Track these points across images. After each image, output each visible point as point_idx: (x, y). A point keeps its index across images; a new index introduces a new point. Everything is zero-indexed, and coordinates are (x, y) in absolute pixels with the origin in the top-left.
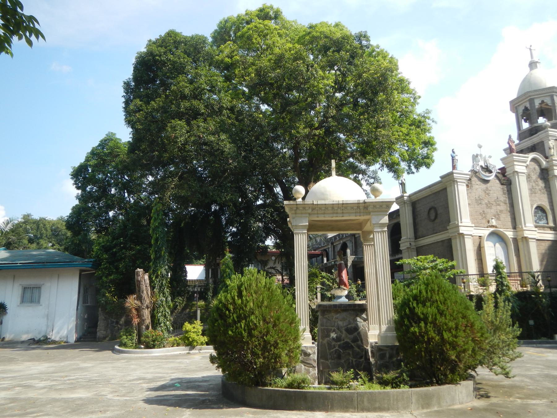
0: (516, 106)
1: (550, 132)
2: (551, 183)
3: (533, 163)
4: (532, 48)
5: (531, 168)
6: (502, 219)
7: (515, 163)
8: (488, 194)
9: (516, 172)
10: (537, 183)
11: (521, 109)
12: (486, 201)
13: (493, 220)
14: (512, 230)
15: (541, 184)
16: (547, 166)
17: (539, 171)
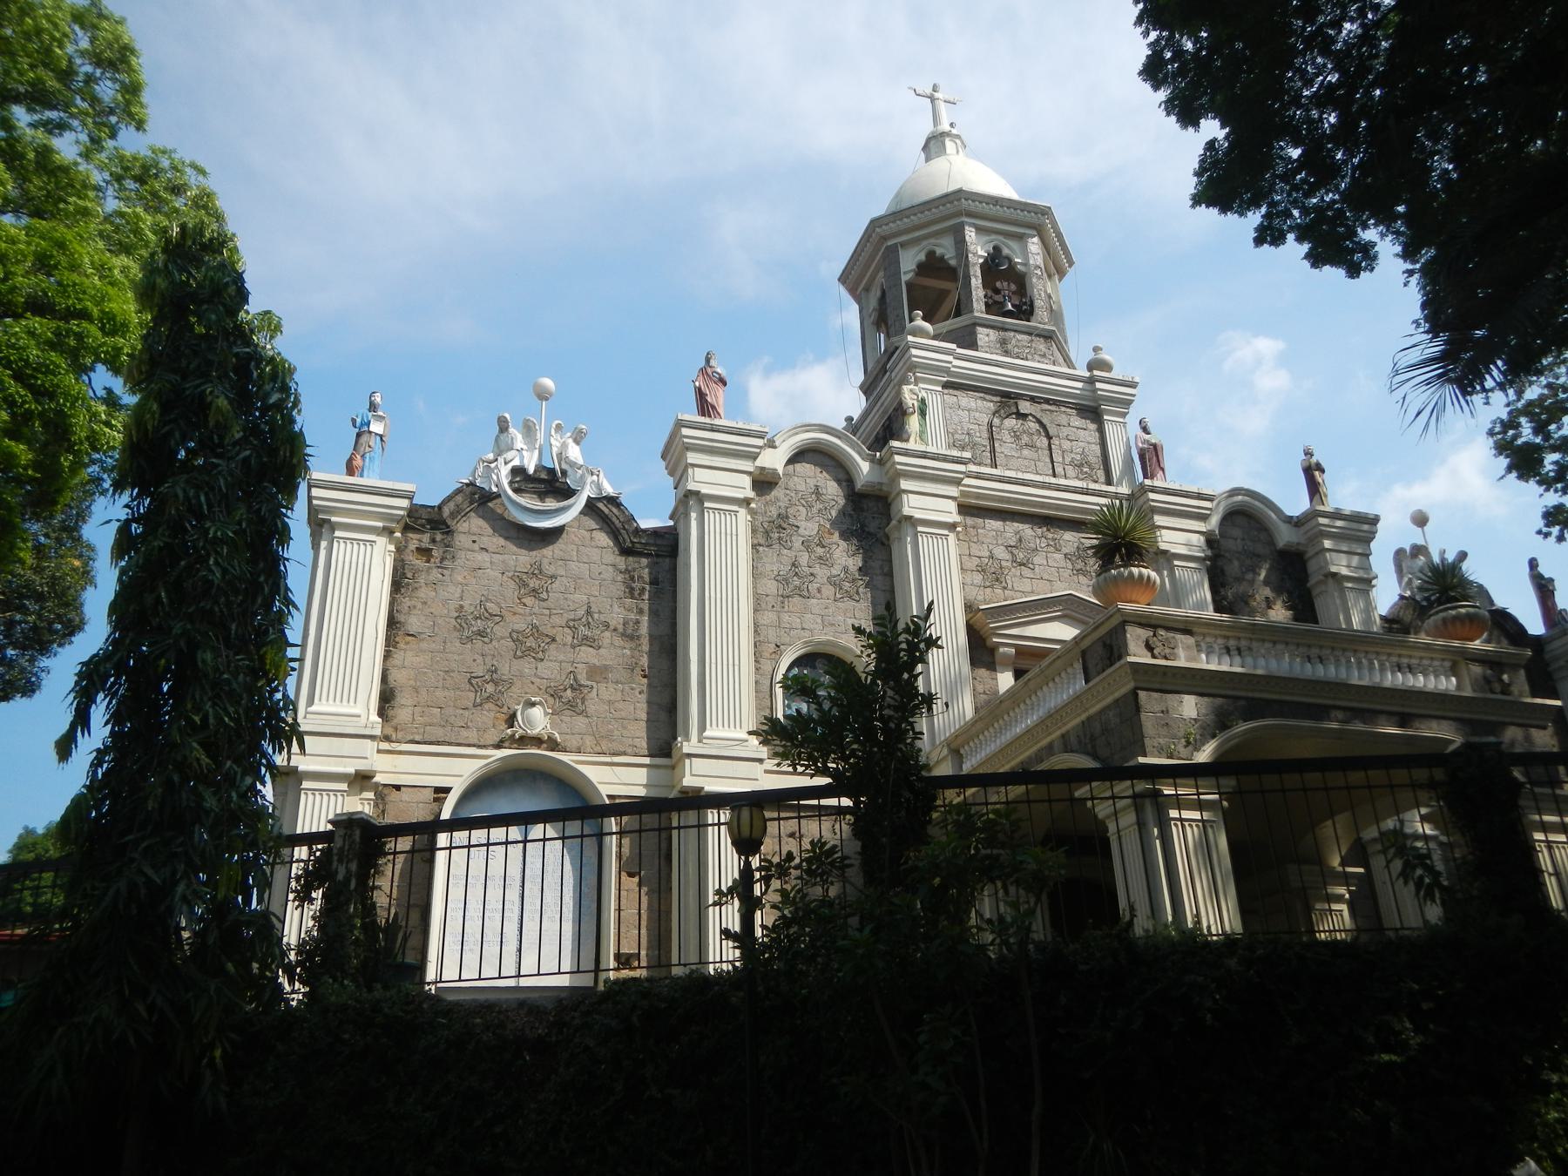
0: (858, 292)
1: (914, 352)
2: (895, 548)
3: (804, 468)
4: (936, 95)
5: (801, 487)
6: (592, 706)
7: (692, 458)
8: (535, 592)
9: (697, 493)
10: (820, 551)
11: (873, 302)
12: (521, 626)
13: (537, 713)
14: (647, 760)
15: (845, 557)
16: (876, 480)
17: (842, 502)
